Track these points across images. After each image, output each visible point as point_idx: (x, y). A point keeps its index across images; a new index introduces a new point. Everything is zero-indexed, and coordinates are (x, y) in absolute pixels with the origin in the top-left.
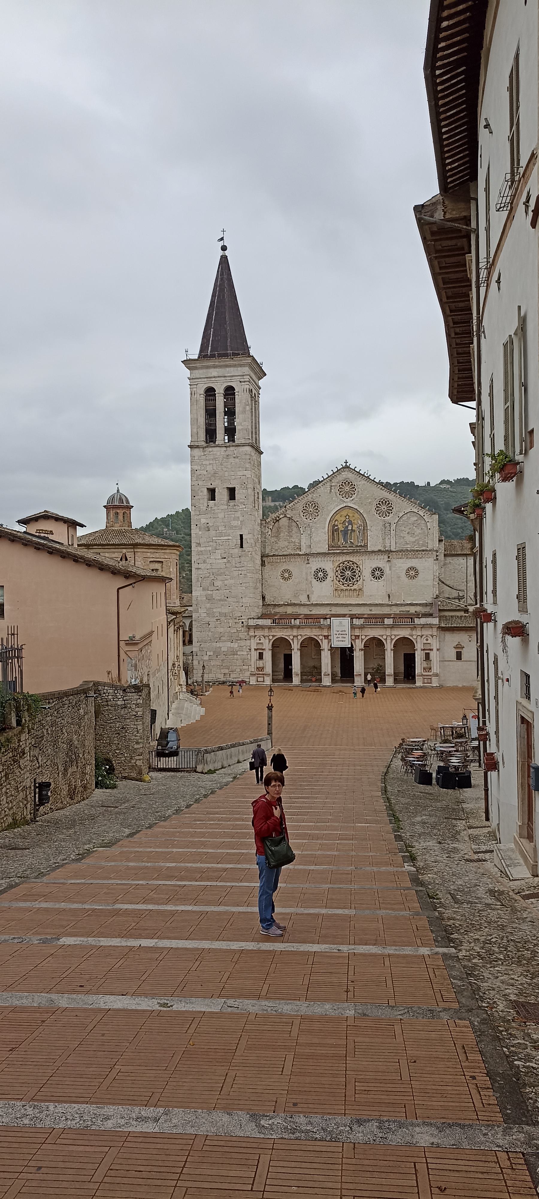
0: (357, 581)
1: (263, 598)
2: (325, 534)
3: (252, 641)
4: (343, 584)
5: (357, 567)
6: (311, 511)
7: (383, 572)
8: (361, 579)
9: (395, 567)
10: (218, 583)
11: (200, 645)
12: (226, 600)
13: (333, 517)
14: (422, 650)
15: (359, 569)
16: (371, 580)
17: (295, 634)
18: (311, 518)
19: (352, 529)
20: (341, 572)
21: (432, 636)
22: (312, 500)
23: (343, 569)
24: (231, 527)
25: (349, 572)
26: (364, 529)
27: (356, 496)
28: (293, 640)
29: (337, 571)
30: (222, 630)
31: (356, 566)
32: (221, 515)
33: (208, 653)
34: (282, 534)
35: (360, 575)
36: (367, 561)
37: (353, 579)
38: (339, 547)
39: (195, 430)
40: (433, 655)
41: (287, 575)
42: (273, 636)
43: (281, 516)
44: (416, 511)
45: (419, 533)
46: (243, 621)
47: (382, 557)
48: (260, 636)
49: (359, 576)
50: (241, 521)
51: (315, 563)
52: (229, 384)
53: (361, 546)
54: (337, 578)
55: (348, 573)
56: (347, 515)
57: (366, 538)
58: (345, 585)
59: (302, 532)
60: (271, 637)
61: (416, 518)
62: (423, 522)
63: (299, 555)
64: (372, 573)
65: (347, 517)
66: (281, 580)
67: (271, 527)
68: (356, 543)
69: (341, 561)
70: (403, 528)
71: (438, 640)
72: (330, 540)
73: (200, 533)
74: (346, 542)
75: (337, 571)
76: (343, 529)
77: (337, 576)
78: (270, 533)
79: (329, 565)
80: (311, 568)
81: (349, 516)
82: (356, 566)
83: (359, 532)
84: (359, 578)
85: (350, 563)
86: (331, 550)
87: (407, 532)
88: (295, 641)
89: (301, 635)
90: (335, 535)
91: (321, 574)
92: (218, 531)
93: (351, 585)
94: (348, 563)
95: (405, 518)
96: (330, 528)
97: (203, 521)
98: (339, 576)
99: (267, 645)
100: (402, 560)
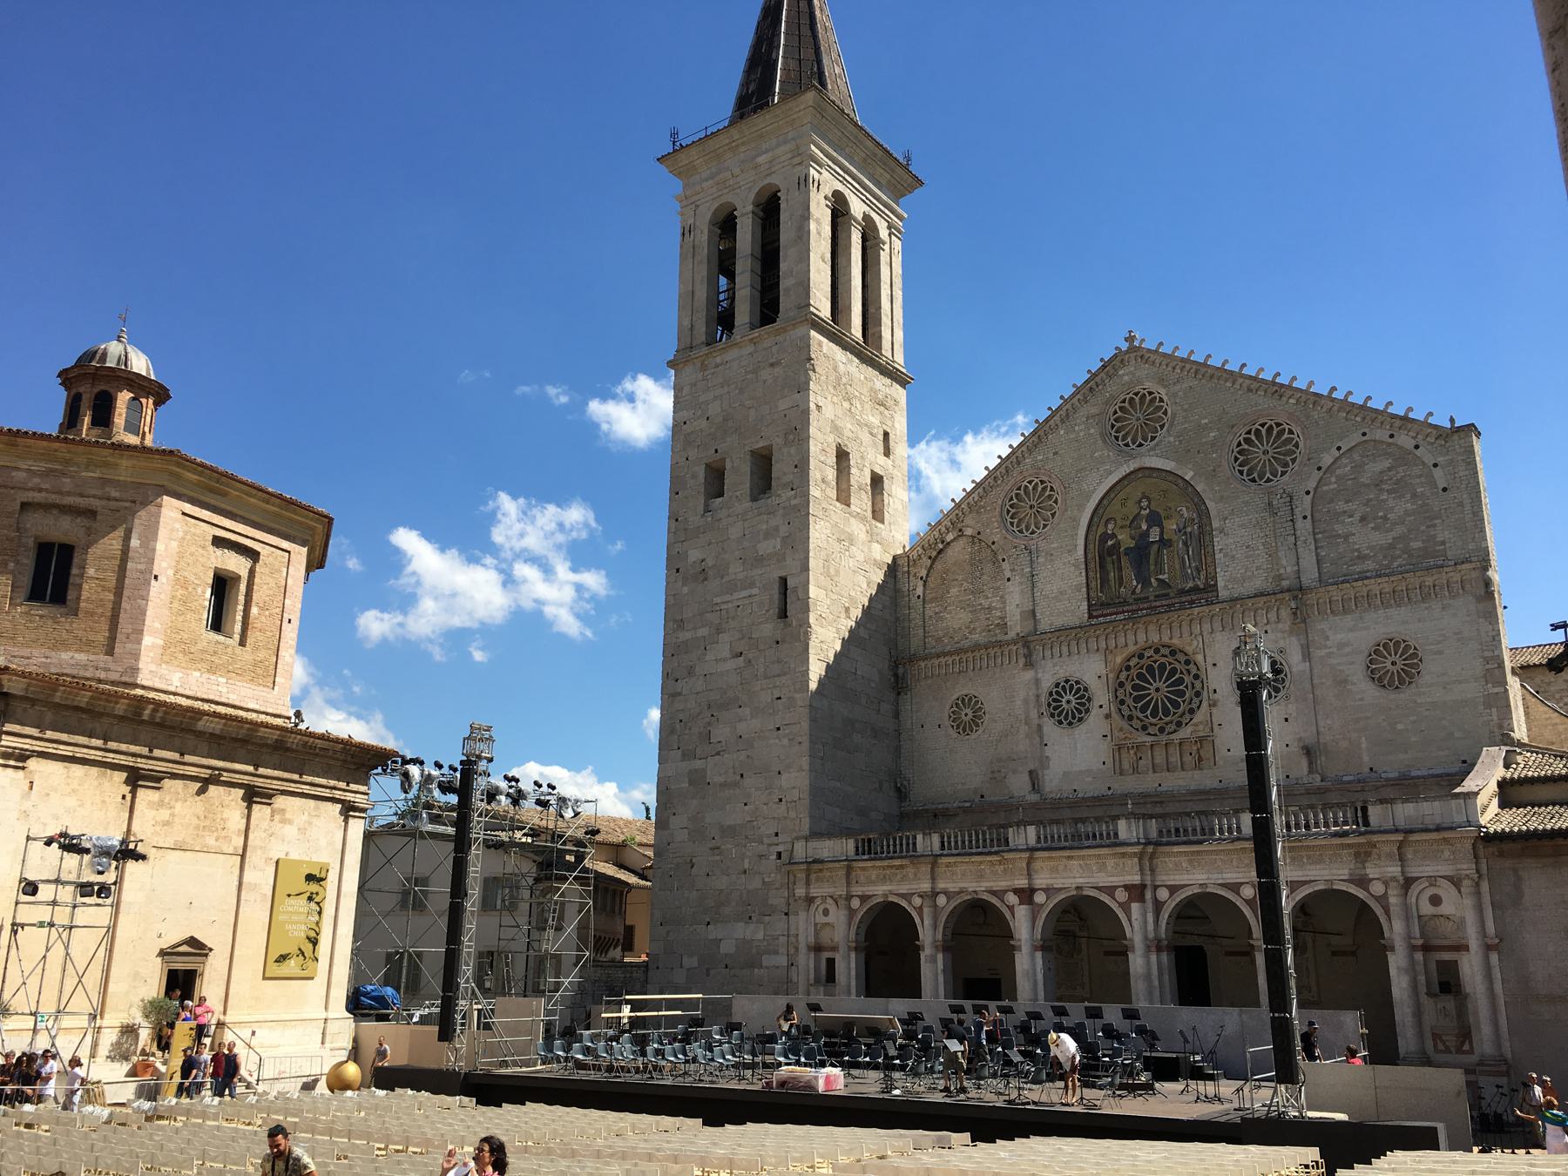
0: (1192, 711)
1: (901, 794)
2: (1076, 567)
3: (802, 915)
4: (1144, 728)
8: (1205, 704)
9: (1326, 647)
10: (721, 733)
11: (668, 933)
12: (735, 785)
14: (1413, 948)
17: (926, 886)
19: (1162, 540)
20: (1136, 688)
21: (1456, 882)
23: (1140, 676)
24: (760, 560)
27: (1168, 431)
28: (920, 910)
29: (1121, 685)
30: (721, 882)
32: (735, 532)
33: (688, 962)
34: (954, 591)
36: (1219, 636)
37: (1176, 705)
38: (1125, 602)
39: (687, 322)
40: (1470, 967)
41: (968, 716)
42: (864, 898)
43: (950, 537)
44: (1381, 434)
45: (1407, 513)
46: (780, 848)
47: (1272, 616)
48: (824, 898)
49: (1198, 694)
50: (783, 538)
52: (766, 182)
53: (1196, 589)
55: (1158, 689)
58: (1151, 730)
59: (1008, 574)
60: (855, 903)
61: (1387, 464)
62: (1416, 470)
63: (1000, 644)
65: (1145, 503)
66: (953, 733)
67: (924, 573)
68: (1181, 584)
69: (1132, 648)
70: (1341, 506)
71: (1487, 899)
73: (685, 590)
74: (1145, 582)
75: (1121, 685)
77: (1122, 702)
78: (920, 591)
79: (1092, 669)
80: (1037, 682)
81: (1149, 501)
82: (1182, 658)
83: (1185, 543)
84: (1196, 700)
85: (1163, 651)
86: (1097, 617)
87: (1357, 516)
88: (926, 910)
89: (946, 893)
90: (1110, 567)
91: (1069, 701)
92: (726, 579)
93: (1173, 727)
94: (1157, 651)
95: (1345, 469)
96: (1091, 546)
97: (694, 555)
98: (1130, 701)
99: (840, 928)
100: (1348, 620)
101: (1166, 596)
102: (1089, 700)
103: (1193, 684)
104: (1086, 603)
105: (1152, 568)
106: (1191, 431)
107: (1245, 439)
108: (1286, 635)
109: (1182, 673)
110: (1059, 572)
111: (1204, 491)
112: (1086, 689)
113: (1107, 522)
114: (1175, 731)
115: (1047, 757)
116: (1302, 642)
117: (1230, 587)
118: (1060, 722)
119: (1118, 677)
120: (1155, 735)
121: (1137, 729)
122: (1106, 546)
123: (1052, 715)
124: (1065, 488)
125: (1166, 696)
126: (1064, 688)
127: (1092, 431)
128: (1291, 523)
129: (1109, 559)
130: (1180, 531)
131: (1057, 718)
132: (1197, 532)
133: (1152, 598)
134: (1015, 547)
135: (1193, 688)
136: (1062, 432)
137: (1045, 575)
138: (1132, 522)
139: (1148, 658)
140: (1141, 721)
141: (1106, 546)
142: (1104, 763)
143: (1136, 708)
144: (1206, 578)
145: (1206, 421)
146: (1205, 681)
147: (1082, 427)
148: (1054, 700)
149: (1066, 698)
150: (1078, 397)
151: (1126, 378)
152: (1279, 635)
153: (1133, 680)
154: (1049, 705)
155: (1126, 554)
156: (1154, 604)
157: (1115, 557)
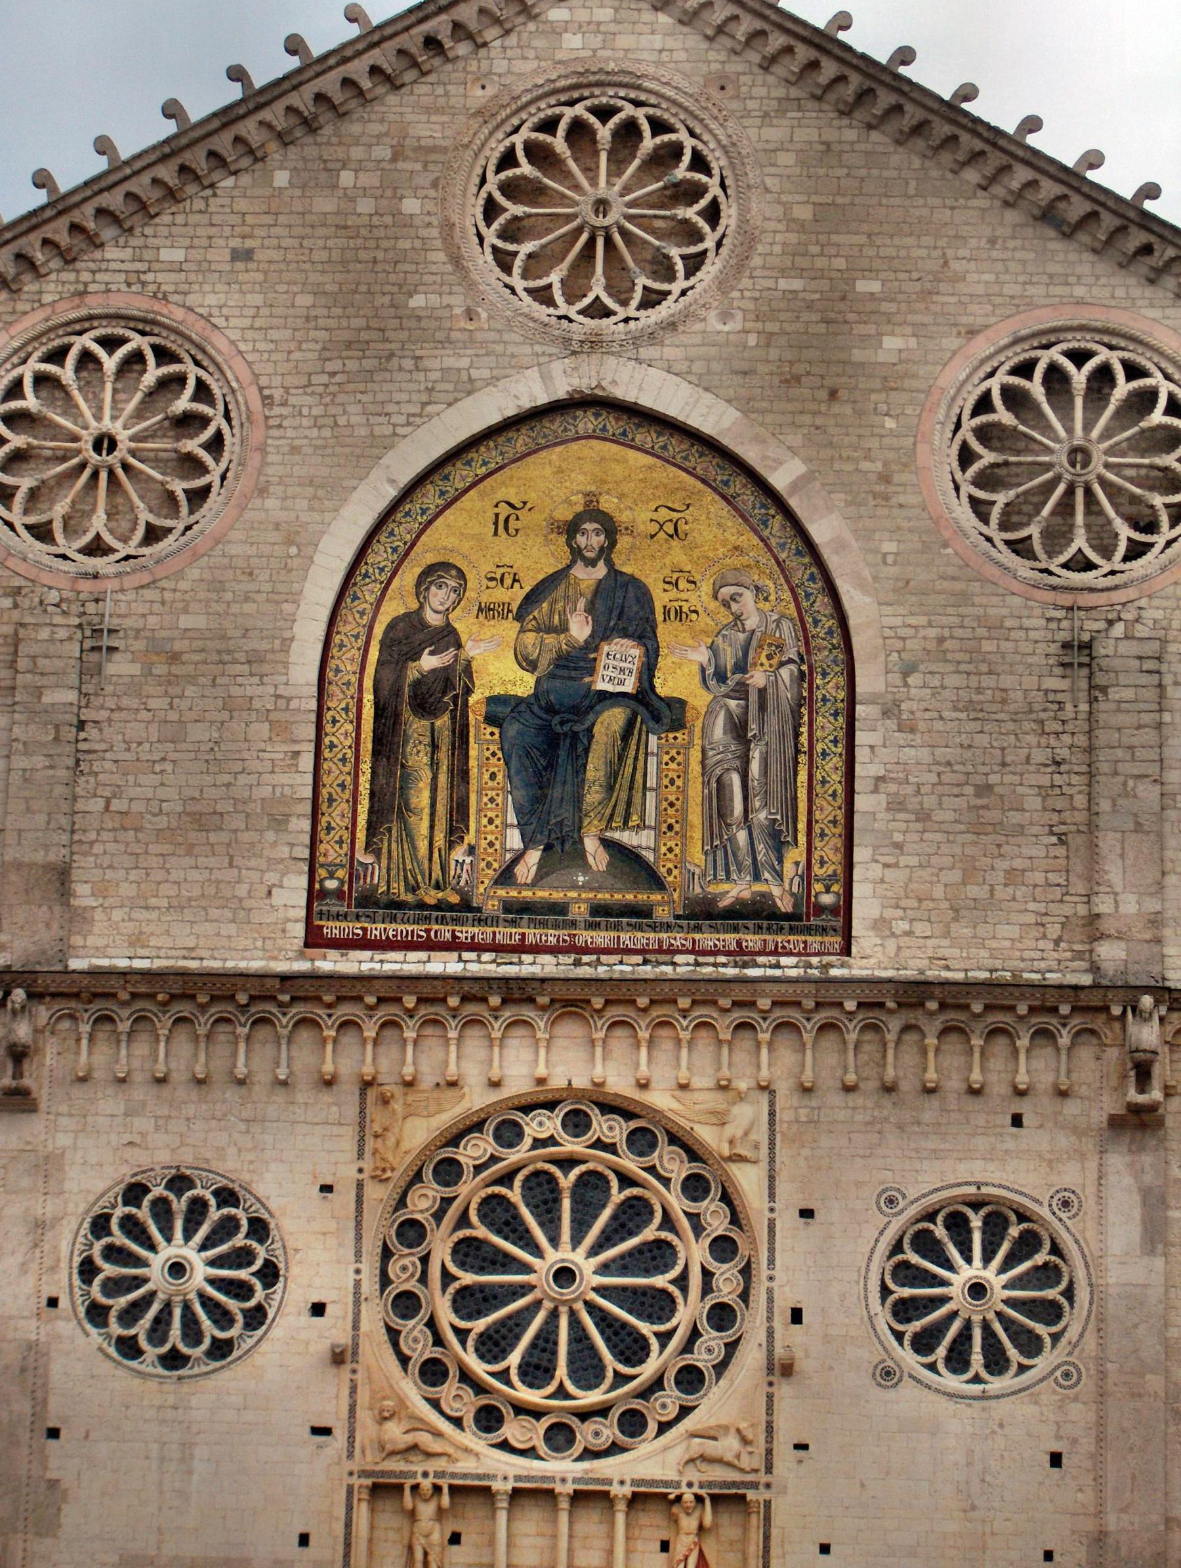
0: (691, 1379)
4: (489, 1419)
5: (695, 1187)
6: (104, 443)
7: (1047, 1274)
8: (750, 1357)
13: (403, 529)
15: (717, 1223)
16: (887, 1375)
18: (98, 523)
22: (137, 304)
25: (586, 1265)
26: (805, 702)
27: (723, 284)
29: (411, 1232)
31: (677, 1167)
35: (727, 1287)
49: (722, 1316)
51: (110, 1104)
54: (413, 1329)
56: (593, 513)
57: (828, 810)
58: (514, 1430)
64: (905, 1273)
65: (591, 539)
69: (476, 1098)
72: (336, 816)
75: (411, 1232)
76: (523, 684)
77: (406, 1304)
83: (739, 729)
84: (712, 1340)
85: (605, 1127)
86: (344, 944)
90: (418, 758)
93: (608, 1431)
94: (577, 1123)
96: (345, 661)
101: (639, 914)
102: (270, 1274)
103: (707, 1274)
104: (303, 881)
105: (593, 796)
106: (810, 306)
107: (1006, 391)
108: (1089, 1145)
109: (668, 1222)
110: (198, 733)
111: (840, 546)
112: (259, 1229)
113: (432, 573)
114: (615, 1449)
115: (53, 1484)
116: (1148, 1178)
117: (902, 926)
118: (129, 1348)
119: (401, 1203)
120: (530, 1453)
121: (457, 1422)
122: (412, 674)
123: (97, 1314)
124: (267, 401)
125: (591, 1307)
126: (162, 1210)
127: (411, 206)
128: (1149, 736)
129: (416, 727)
130: (721, 677)
131: (116, 1329)
132: (787, 694)
133: (579, 911)
134: (18, 591)
135: (707, 1289)
136: (281, 178)
137: (135, 730)
138: (532, 599)
139: (538, 1143)
140: (480, 1388)
141: (412, 674)
142: (304, 1540)
143: (462, 1334)
144: (807, 877)
145: (875, 287)
146: (761, 1270)
147: (369, 179)
148: (114, 1254)
149: (167, 1252)
150: (375, 57)
151: (573, 42)
152: (1064, 1141)
153: (463, 1221)
154: (88, 1270)
155: (491, 719)
156: (586, 936)
157: (443, 722)
